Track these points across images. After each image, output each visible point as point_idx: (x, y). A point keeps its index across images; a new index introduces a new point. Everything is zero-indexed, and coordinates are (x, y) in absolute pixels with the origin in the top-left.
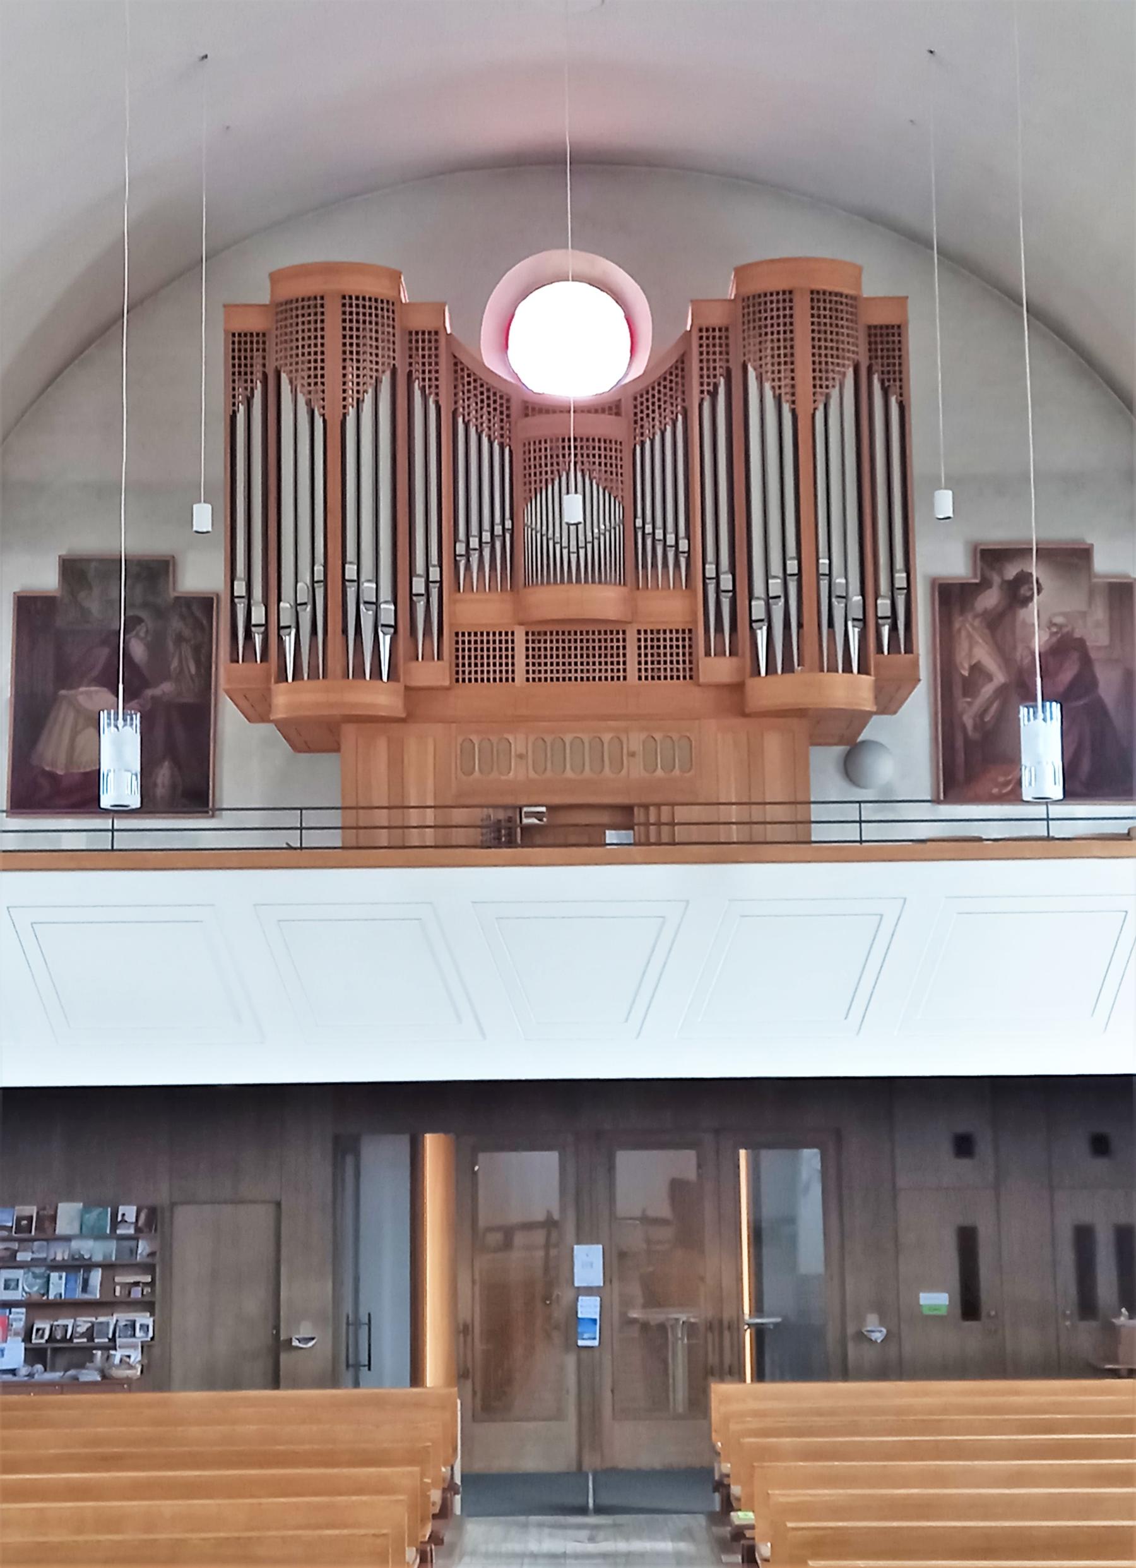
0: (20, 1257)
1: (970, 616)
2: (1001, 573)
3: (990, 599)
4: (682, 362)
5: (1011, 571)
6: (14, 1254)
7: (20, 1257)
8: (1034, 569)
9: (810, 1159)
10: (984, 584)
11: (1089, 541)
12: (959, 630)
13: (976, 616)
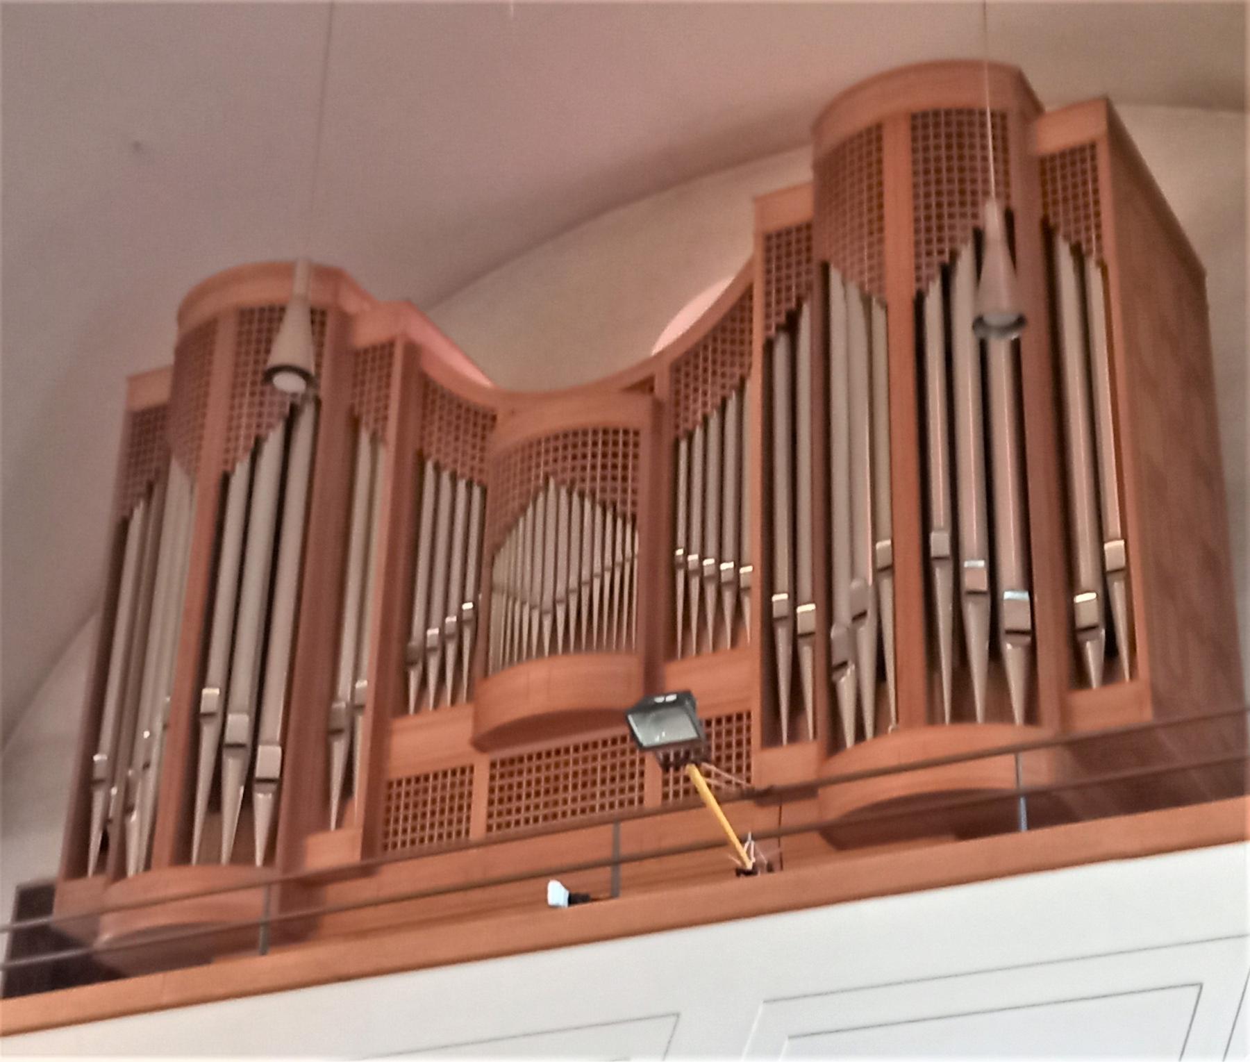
4: (748, 295)
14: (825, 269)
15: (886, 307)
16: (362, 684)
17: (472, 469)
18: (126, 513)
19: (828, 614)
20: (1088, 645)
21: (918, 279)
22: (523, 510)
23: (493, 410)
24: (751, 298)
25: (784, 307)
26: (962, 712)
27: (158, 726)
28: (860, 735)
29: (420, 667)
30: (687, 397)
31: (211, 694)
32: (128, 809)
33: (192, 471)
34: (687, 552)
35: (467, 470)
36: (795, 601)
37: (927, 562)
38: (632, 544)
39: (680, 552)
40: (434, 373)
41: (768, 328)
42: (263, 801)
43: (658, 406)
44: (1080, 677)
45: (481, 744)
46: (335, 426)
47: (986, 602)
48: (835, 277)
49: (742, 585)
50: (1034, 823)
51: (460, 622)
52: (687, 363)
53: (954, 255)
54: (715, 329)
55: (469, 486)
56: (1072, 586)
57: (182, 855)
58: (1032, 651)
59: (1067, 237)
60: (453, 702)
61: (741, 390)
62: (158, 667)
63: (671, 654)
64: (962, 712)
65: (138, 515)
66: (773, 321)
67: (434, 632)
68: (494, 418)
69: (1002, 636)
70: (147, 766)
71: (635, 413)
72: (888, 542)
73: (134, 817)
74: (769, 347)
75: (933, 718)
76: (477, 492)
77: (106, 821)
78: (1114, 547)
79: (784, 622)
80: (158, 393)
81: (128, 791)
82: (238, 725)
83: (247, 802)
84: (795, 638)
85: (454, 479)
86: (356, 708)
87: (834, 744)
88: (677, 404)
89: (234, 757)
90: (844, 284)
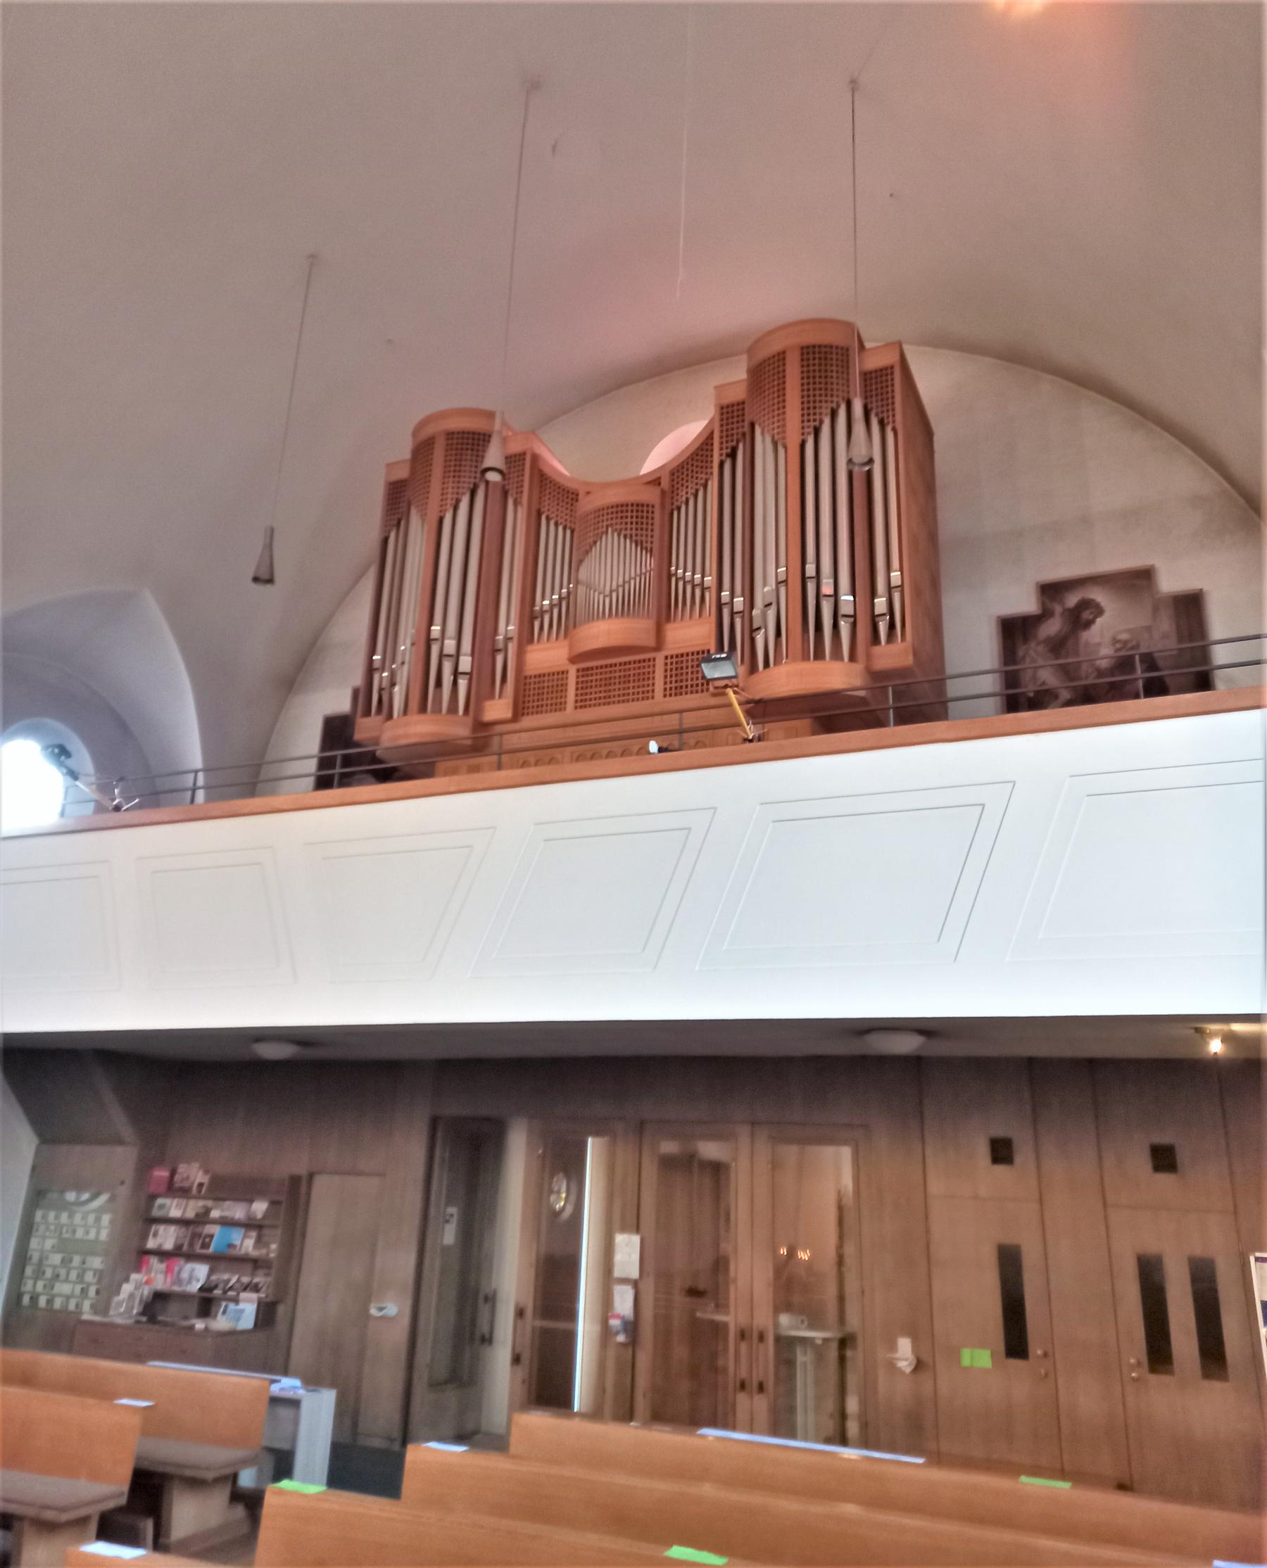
0: (215, 1214)
1: (1033, 644)
2: (1061, 602)
3: (1052, 627)
5: (1072, 600)
6: (207, 1211)
7: (215, 1214)
8: (1098, 595)
9: (846, 1152)
10: (1044, 615)
11: (1151, 563)
12: (1024, 657)
13: (1038, 644)
14: (752, 426)
15: (785, 448)
16: (511, 628)
17: (566, 520)
18: (387, 535)
19: (751, 604)
20: (881, 623)
21: (803, 434)
22: (595, 543)
23: (576, 490)
24: (712, 439)
25: (730, 444)
26: (819, 655)
27: (408, 642)
28: (767, 664)
29: (539, 619)
30: (678, 489)
31: (436, 628)
32: (393, 684)
33: (423, 517)
34: (677, 569)
35: (562, 520)
36: (732, 595)
37: (804, 579)
38: (650, 563)
39: (673, 568)
40: (546, 470)
41: (721, 455)
42: (463, 683)
43: (663, 492)
44: (875, 639)
45: (573, 660)
46: (496, 496)
47: (832, 599)
48: (758, 430)
49: (705, 586)
50: (897, 723)
51: (560, 599)
52: (678, 471)
53: (821, 422)
54: (692, 454)
55: (565, 529)
56: (873, 594)
57: (423, 709)
58: (854, 625)
59: (877, 415)
60: (557, 638)
61: (705, 486)
62: (407, 617)
63: (668, 619)
64: (819, 655)
65: (393, 535)
66: (724, 451)
67: (546, 602)
68: (577, 495)
69: (840, 618)
70: (403, 663)
71: (650, 496)
72: (785, 569)
73: (397, 689)
74: (721, 464)
75: (805, 657)
76: (568, 532)
77: (381, 689)
78: (895, 575)
79: (727, 606)
80: (403, 473)
81: (393, 674)
82: (450, 646)
83: (455, 683)
84: (732, 614)
85: (556, 524)
86: (508, 639)
87: (753, 669)
88: (673, 492)
89: (448, 661)
90: (763, 434)
